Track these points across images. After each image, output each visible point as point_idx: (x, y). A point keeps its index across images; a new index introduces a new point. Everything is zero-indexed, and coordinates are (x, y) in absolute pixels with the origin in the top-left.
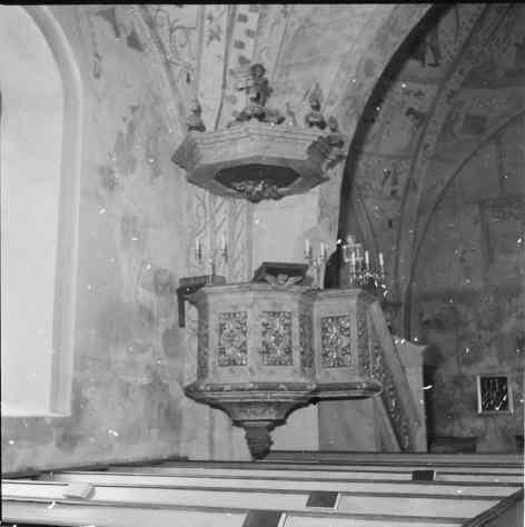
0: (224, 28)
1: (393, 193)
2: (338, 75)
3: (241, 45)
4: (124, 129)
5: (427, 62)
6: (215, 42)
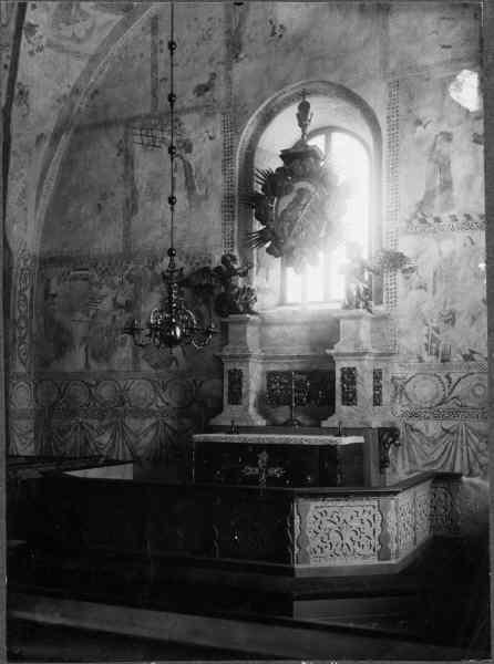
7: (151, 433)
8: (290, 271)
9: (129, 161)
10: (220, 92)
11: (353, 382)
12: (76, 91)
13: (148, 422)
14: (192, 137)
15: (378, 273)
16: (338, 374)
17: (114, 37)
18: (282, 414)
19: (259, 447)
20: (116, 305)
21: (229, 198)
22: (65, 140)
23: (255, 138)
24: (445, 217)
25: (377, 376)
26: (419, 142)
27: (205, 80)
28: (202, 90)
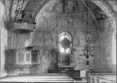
0: (17, 2)
2: (35, 14)
6: (15, 4)
9: (44, 36)
10: (55, 30)
11: (72, 61)
13: (47, 65)
14: (52, 34)
18: (64, 64)
19: (66, 67)
20: (42, 52)
22: (36, 32)
23: (59, 35)
24: (79, 46)
27: (54, 28)
28: (53, 29)
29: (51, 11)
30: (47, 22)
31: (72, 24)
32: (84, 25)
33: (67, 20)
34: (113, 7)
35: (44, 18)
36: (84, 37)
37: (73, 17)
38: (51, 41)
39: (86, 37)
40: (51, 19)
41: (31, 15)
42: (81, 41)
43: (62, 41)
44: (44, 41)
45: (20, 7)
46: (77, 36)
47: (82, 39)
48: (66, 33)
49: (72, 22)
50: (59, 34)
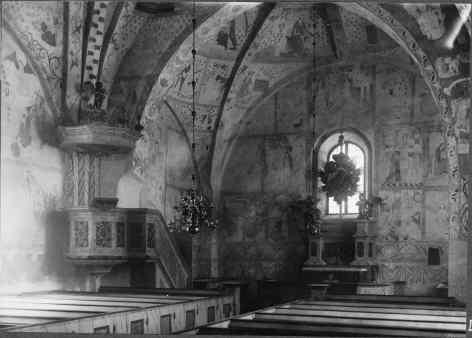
0: (80, 58)
1: (209, 128)
3: (90, 68)
4: (24, 120)
5: (229, 46)
6: (75, 67)
7: (273, 269)
8: (331, 199)
9: (264, 153)
10: (304, 128)
11: (363, 248)
12: (241, 122)
14: (292, 145)
15: (371, 205)
16: (356, 246)
17: (259, 101)
18: (333, 260)
19: (330, 272)
20: (257, 214)
21: (308, 172)
22: (235, 141)
23: (319, 147)
24: (397, 185)
25: (370, 244)
26: (387, 153)
28: (296, 126)
29: (282, 54)
30: (276, 99)
31: (368, 97)
32: (417, 94)
33: (347, 84)
34: (420, 21)
35: (261, 85)
36: (418, 148)
37: (374, 67)
38: (287, 170)
39: (426, 148)
40: (287, 87)
41: (135, 93)
42: (403, 167)
43: (325, 168)
44: (265, 171)
45: (95, 72)
46: (387, 143)
47: (411, 155)
48: (341, 138)
49: (368, 88)
50: (318, 140)
